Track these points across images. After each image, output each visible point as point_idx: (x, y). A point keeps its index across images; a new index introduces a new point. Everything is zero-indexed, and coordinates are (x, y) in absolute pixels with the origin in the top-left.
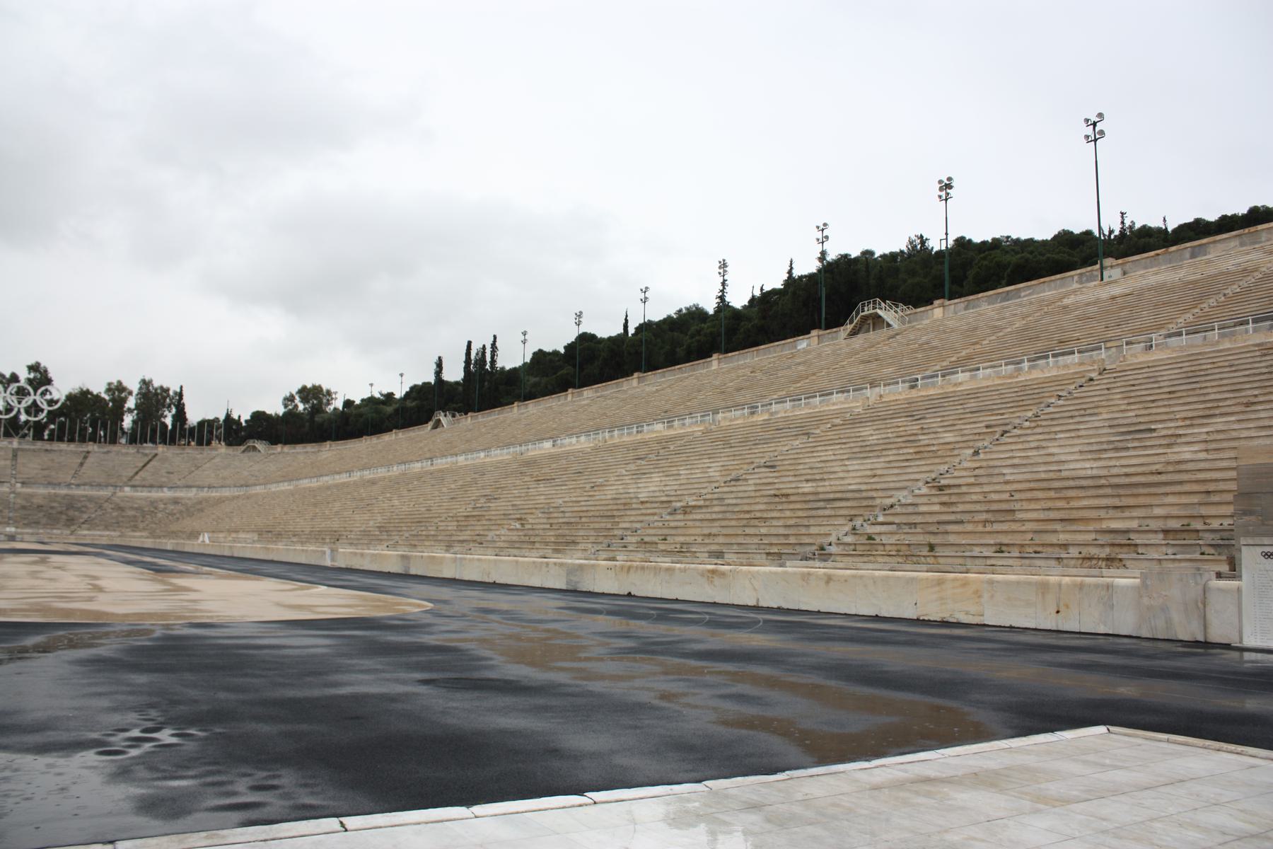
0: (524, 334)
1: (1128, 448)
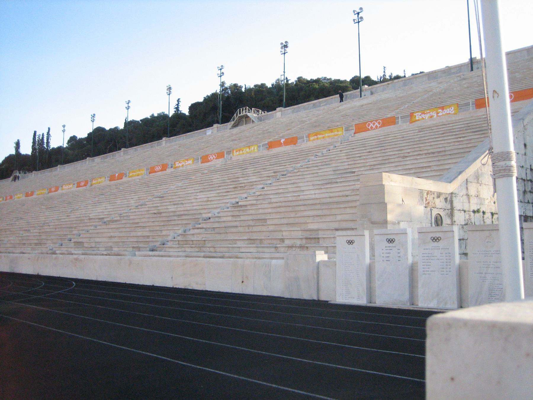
0: (64, 126)
1: (337, 182)
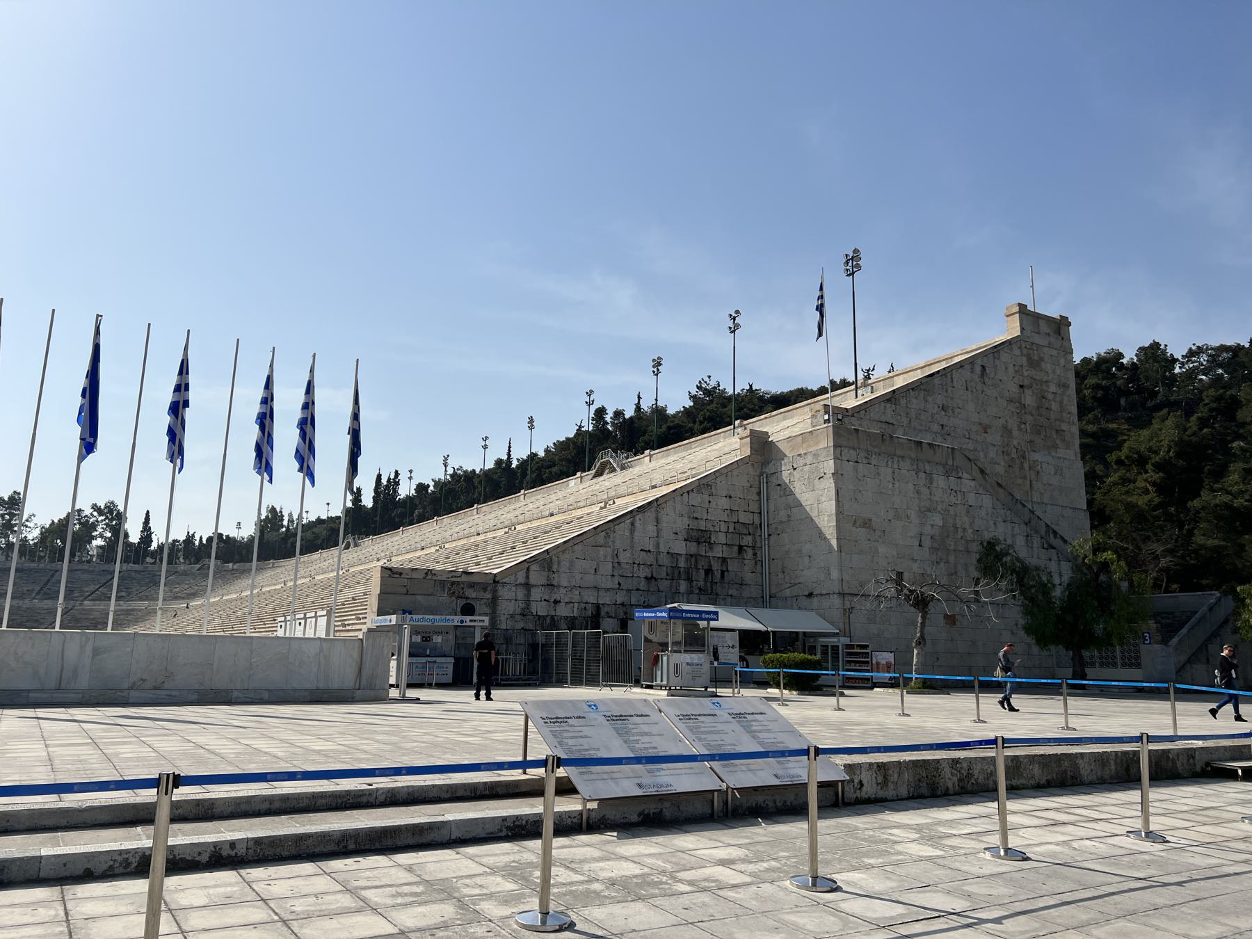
0: (411, 471)
